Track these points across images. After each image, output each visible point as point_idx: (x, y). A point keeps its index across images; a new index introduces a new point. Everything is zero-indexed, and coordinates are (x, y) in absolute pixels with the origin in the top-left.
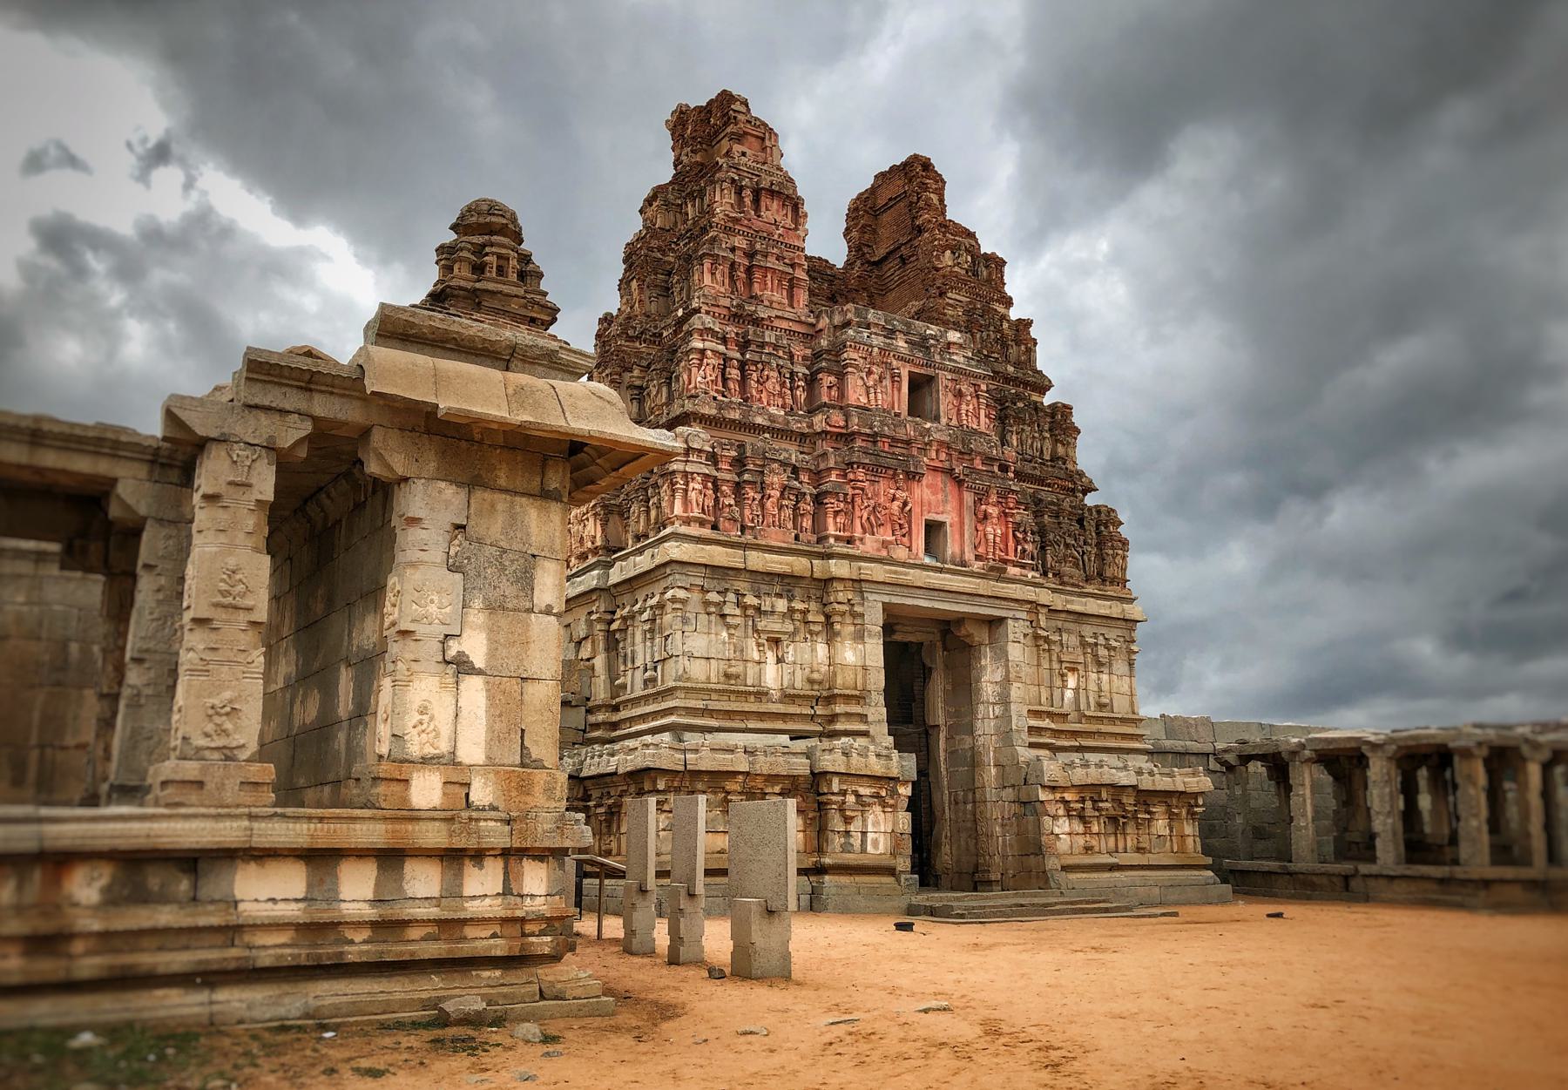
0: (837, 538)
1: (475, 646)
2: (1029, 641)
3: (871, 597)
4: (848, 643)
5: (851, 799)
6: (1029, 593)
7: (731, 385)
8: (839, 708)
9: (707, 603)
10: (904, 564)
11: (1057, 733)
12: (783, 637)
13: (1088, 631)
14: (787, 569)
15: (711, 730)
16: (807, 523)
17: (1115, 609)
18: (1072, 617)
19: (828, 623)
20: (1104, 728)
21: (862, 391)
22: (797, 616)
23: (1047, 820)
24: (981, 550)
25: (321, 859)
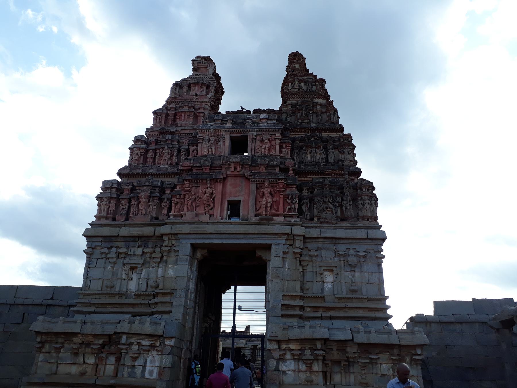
0: (175, 216)
2: (290, 256)
3: (184, 241)
4: (170, 266)
5: (135, 347)
6: (286, 229)
7: (148, 160)
8: (157, 300)
9: (102, 253)
10: (208, 223)
11: (316, 308)
12: (139, 266)
13: (342, 248)
14: (140, 233)
15: (90, 313)
16: (165, 211)
17: (360, 234)
18: (326, 241)
19: (162, 257)
20: (350, 305)
21: (206, 149)
22: (148, 255)
23: (272, 363)
24: (259, 212)
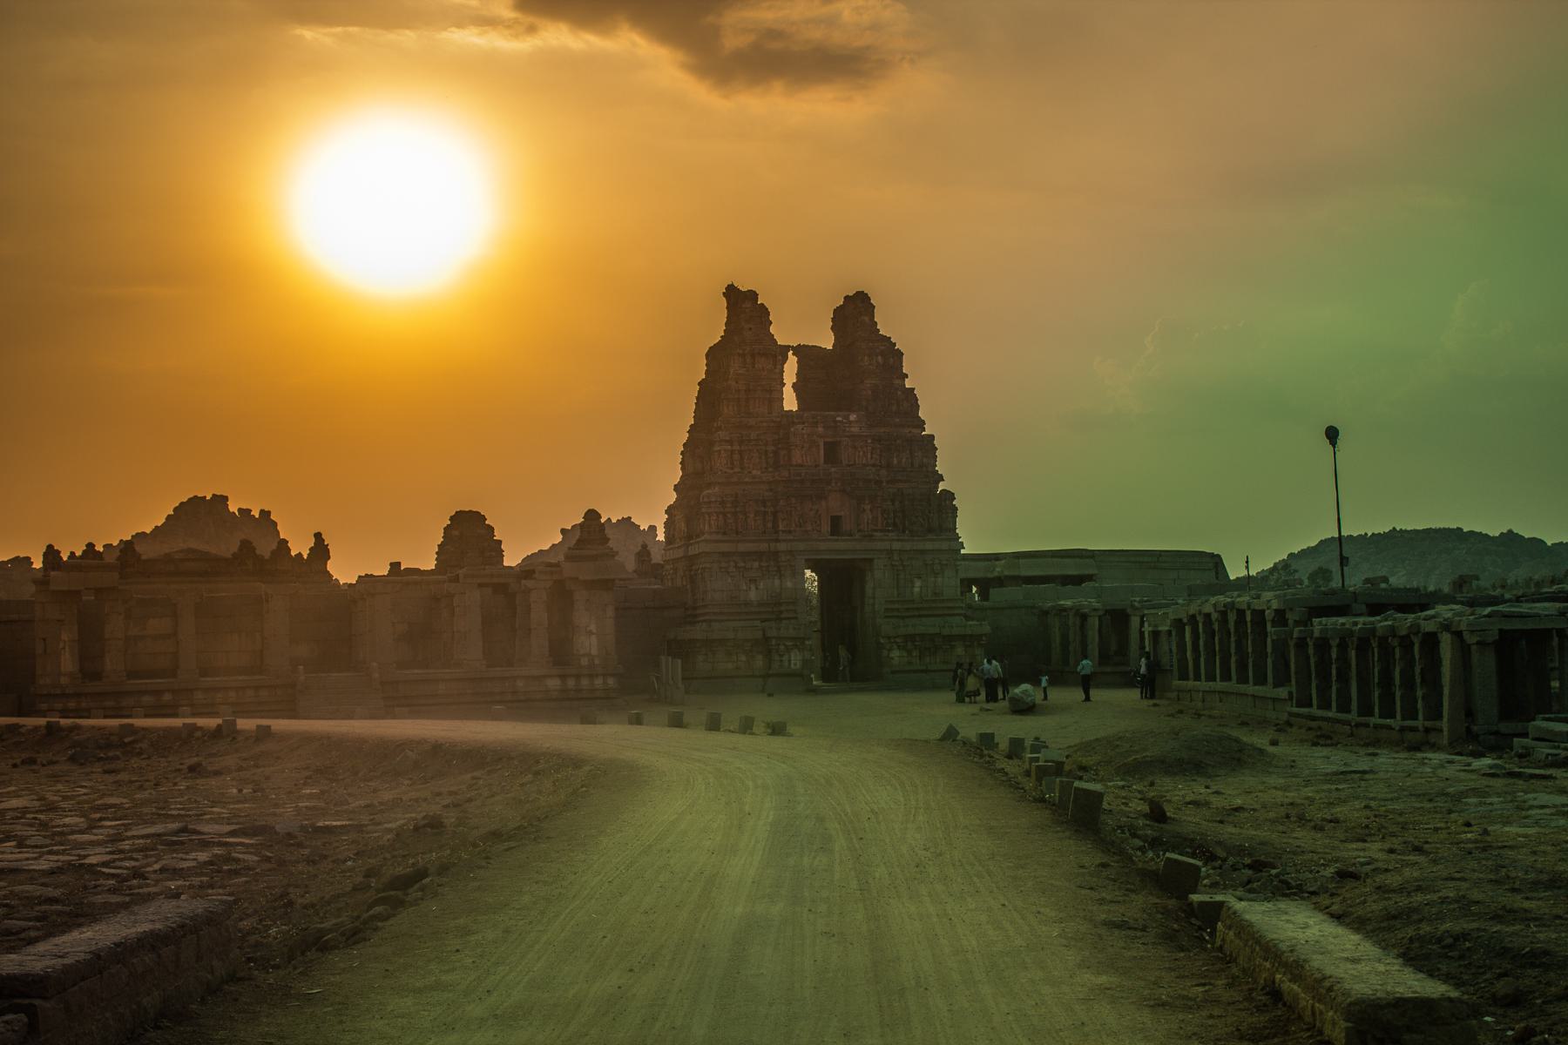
1: (593, 628)
16: (770, 525)
17: (945, 546)
23: (885, 653)
25: (563, 677)
